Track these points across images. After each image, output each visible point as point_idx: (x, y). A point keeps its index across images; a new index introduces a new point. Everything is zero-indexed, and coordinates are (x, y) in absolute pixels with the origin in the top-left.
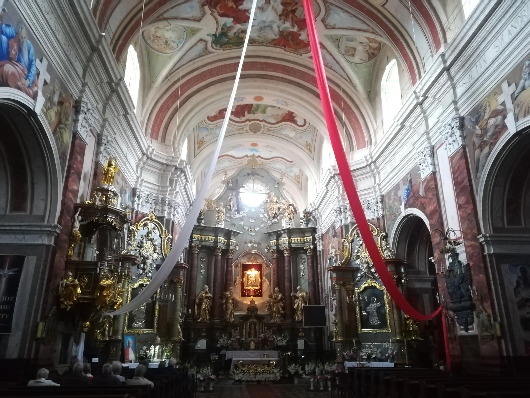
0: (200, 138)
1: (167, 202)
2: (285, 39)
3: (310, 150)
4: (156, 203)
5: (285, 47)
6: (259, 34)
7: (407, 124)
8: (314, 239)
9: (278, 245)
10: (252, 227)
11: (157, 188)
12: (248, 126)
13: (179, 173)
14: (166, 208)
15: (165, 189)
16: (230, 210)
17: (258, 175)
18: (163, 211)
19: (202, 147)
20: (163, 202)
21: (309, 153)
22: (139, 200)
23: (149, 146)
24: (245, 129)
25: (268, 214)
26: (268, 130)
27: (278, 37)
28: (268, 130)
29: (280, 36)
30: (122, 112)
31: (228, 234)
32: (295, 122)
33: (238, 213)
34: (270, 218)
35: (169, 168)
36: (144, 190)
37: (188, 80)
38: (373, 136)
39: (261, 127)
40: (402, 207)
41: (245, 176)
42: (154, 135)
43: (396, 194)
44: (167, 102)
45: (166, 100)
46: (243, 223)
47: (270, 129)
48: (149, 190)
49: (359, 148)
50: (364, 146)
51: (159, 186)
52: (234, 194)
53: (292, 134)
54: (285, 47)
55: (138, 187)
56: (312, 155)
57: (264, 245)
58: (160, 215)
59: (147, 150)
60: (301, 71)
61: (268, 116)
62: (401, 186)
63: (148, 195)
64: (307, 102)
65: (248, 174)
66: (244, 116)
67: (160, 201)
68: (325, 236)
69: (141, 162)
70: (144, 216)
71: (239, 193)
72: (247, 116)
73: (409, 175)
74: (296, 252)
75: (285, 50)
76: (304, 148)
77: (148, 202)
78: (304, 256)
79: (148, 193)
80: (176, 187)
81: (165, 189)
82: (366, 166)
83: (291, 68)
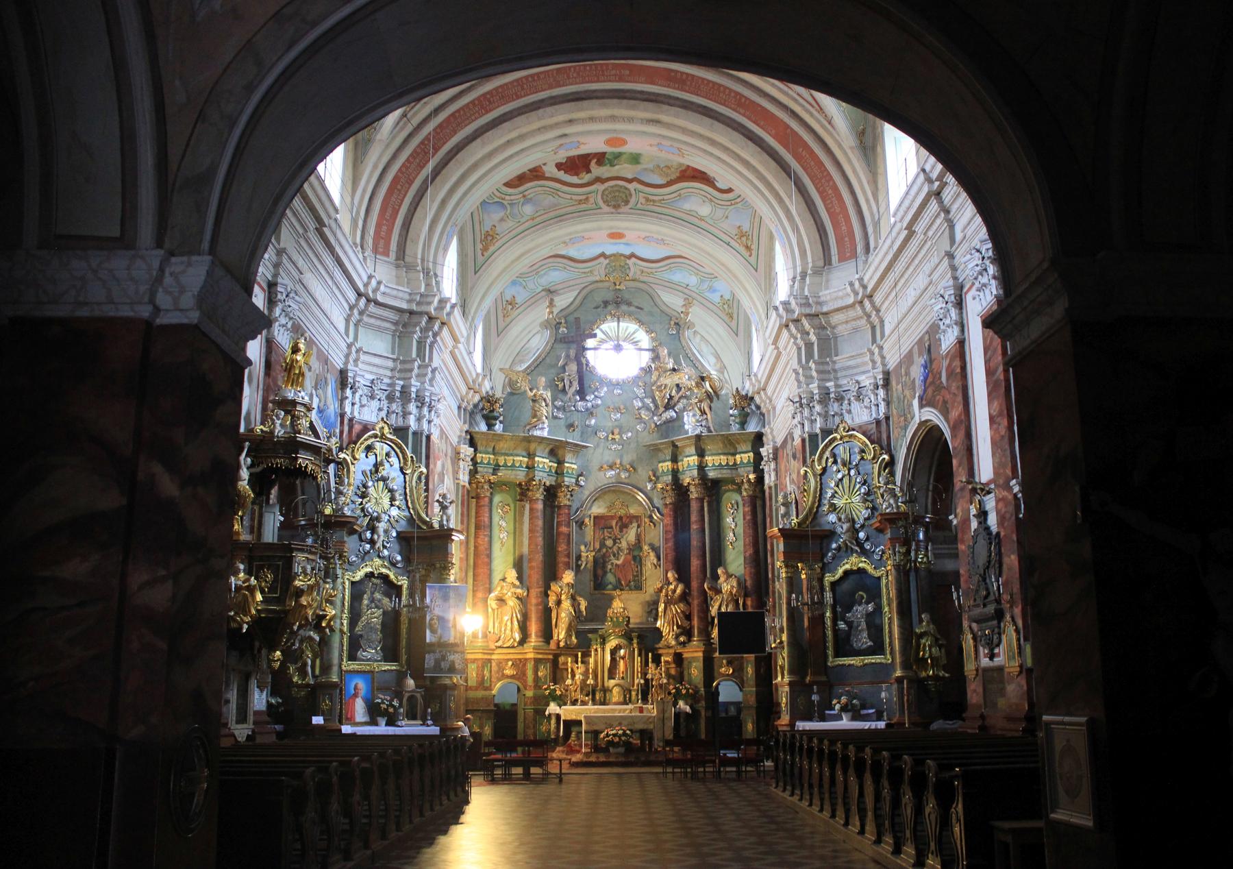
0: (487, 227)
1: (413, 395)
3: (748, 248)
4: (390, 398)
7: (920, 227)
8: (758, 458)
9: (675, 473)
10: (616, 431)
11: (390, 364)
13: (436, 328)
14: (412, 407)
15: (407, 366)
16: (564, 390)
17: (629, 304)
18: (405, 414)
20: (405, 392)
21: (746, 254)
22: (354, 393)
23: (370, 277)
24: (592, 200)
25: (654, 401)
26: (647, 200)
28: (647, 200)
30: (312, 225)
31: (556, 451)
33: (583, 399)
34: (657, 407)
35: (415, 319)
36: (363, 374)
37: (453, 115)
38: (870, 230)
39: (631, 195)
40: (916, 403)
41: (597, 308)
42: (380, 248)
43: (907, 374)
44: (407, 168)
45: (403, 165)
46: (593, 422)
48: (374, 369)
49: (842, 259)
50: (854, 255)
51: (394, 360)
52: (572, 353)
53: (705, 210)
55: (350, 367)
56: (753, 260)
57: (644, 472)
58: (400, 423)
59: (366, 285)
61: (646, 169)
62: (916, 356)
63: (372, 382)
64: (726, 149)
65: (606, 303)
66: (589, 171)
67: (398, 394)
68: (780, 453)
69: (356, 312)
70: (366, 428)
71: (585, 349)
73: (927, 337)
74: (713, 488)
76: (733, 243)
77: (372, 397)
78: (736, 497)
79: (371, 377)
80: (431, 359)
81: (407, 366)
82: (852, 306)
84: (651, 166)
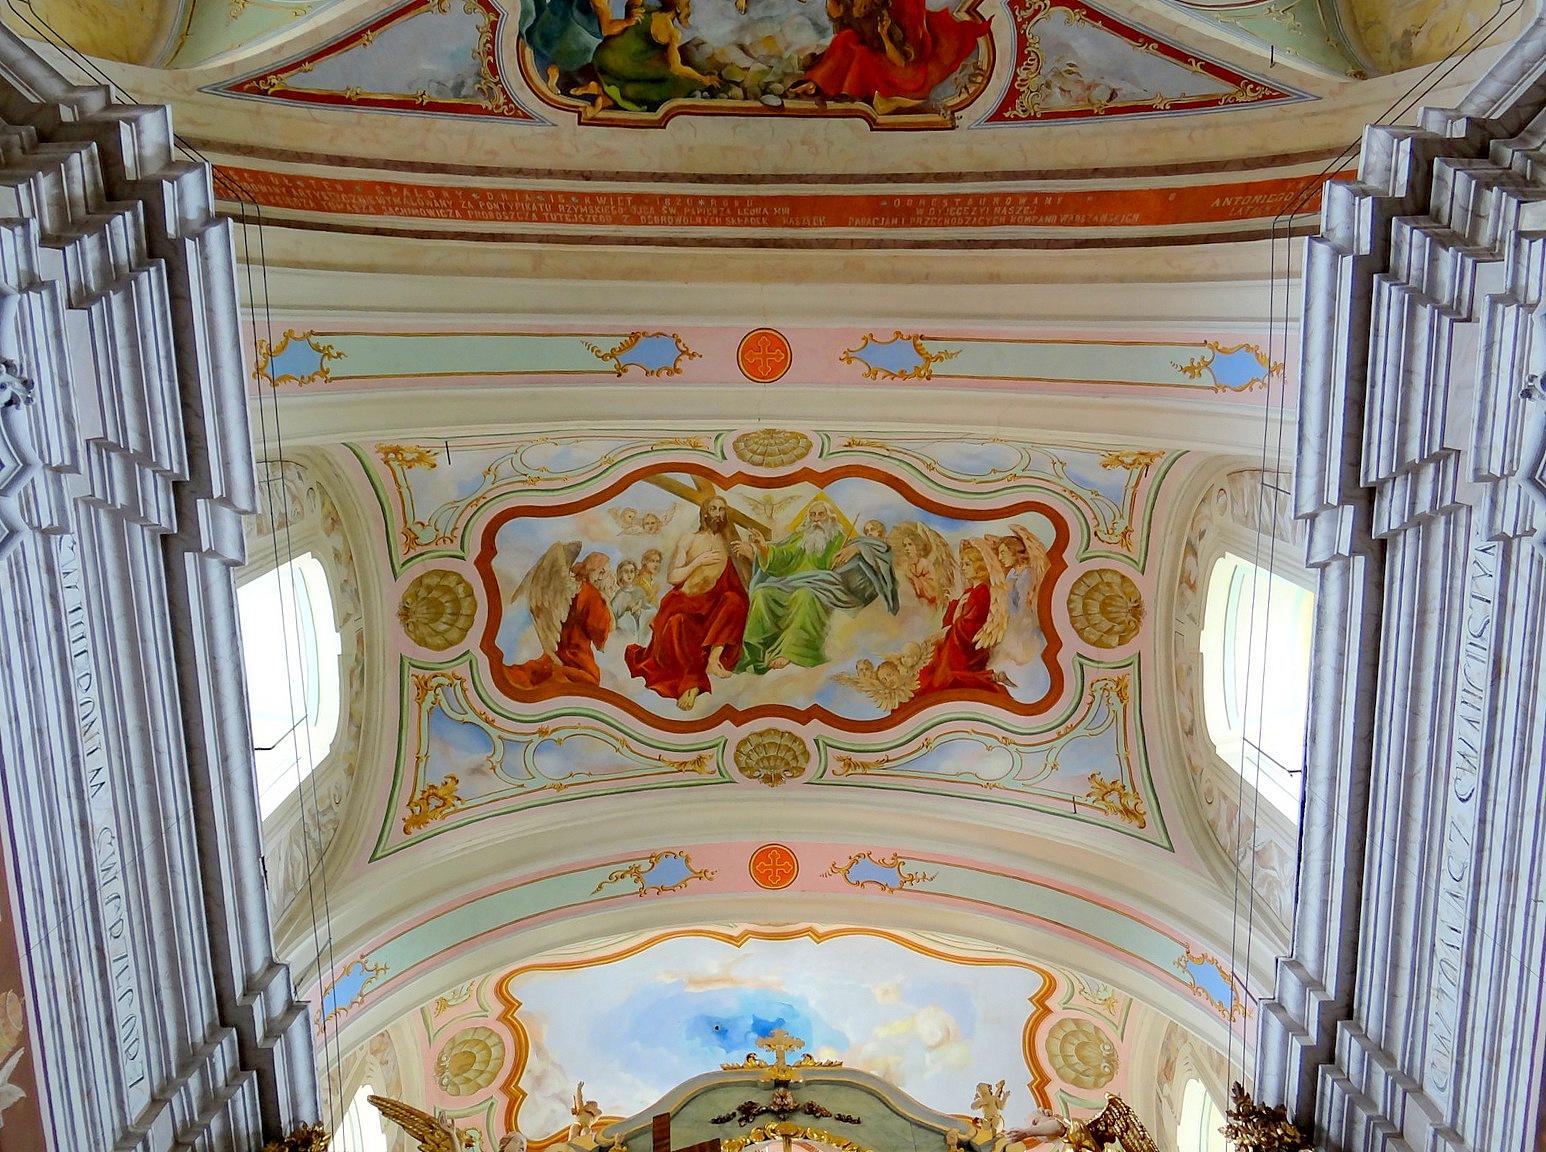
0: (435, 776)
2: (861, 38)
5: (869, 100)
6: (743, 28)
12: (730, 751)
19: (434, 825)
24: (710, 765)
26: (849, 764)
27: (827, 41)
29: (841, 23)
32: (992, 690)
47: (857, 758)
54: (869, 100)
56: (1153, 830)
60: (965, 197)
61: (838, 679)
66: (704, 687)
72: (727, 686)
75: (875, 126)
83: (917, 198)
84: (849, 666)
